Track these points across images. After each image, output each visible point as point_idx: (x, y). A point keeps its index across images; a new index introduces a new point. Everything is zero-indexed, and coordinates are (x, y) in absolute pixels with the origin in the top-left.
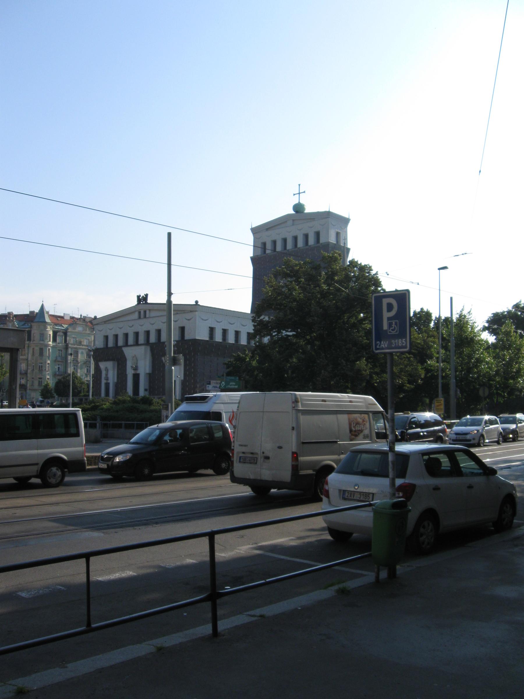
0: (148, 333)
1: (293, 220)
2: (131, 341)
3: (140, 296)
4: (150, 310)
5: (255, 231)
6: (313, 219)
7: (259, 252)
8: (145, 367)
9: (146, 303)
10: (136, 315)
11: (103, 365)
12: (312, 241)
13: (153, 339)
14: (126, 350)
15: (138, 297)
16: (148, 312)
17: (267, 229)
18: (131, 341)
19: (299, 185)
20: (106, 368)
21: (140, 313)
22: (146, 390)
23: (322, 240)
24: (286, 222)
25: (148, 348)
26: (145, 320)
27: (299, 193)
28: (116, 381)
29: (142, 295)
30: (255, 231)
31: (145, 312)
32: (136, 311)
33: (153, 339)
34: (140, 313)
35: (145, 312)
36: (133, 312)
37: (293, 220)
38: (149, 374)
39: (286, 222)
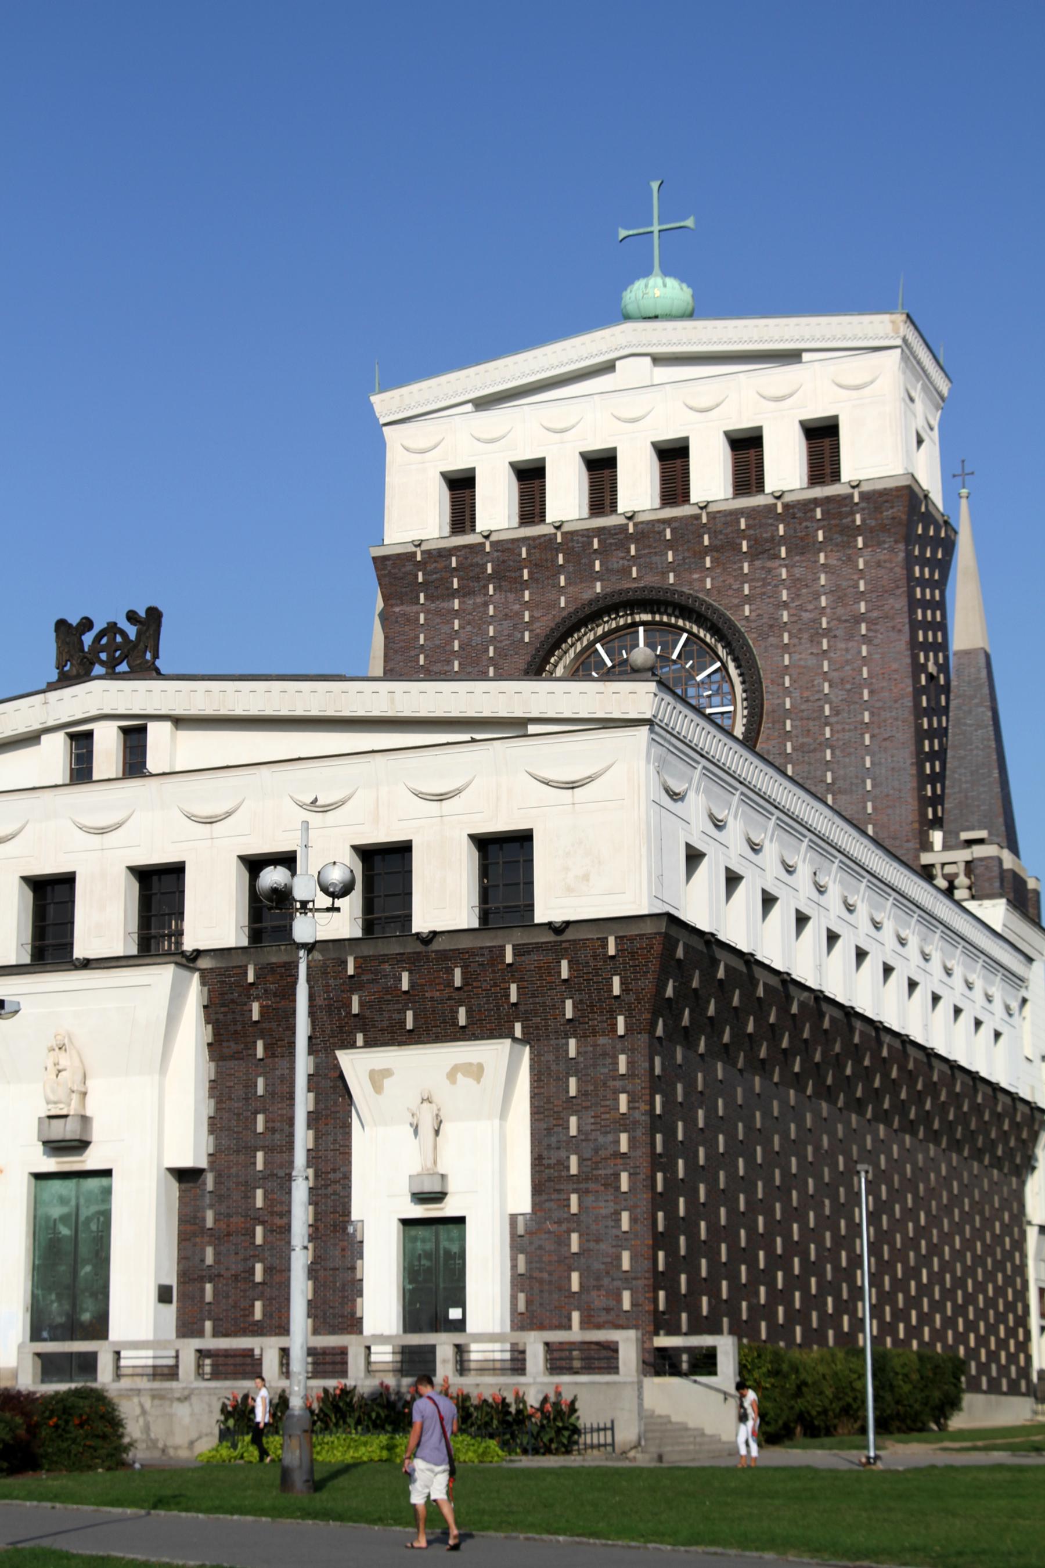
0: (159, 889)
3: (87, 624)
4: (179, 722)
6: (793, 356)
12: (785, 469)
13: (214, 918)
15: (67, 633)
17: (482, 403)
21: (82, 742)
22: (164, 1295)
24: (608, 367)
25: (194, 993)
29: (107, 609)
31: (134, 736)
33: (214, 918)
34: (82, 742)
35: (134, 736)
36: (32, 739)
38: (184, 1176)
39: (608, 367)
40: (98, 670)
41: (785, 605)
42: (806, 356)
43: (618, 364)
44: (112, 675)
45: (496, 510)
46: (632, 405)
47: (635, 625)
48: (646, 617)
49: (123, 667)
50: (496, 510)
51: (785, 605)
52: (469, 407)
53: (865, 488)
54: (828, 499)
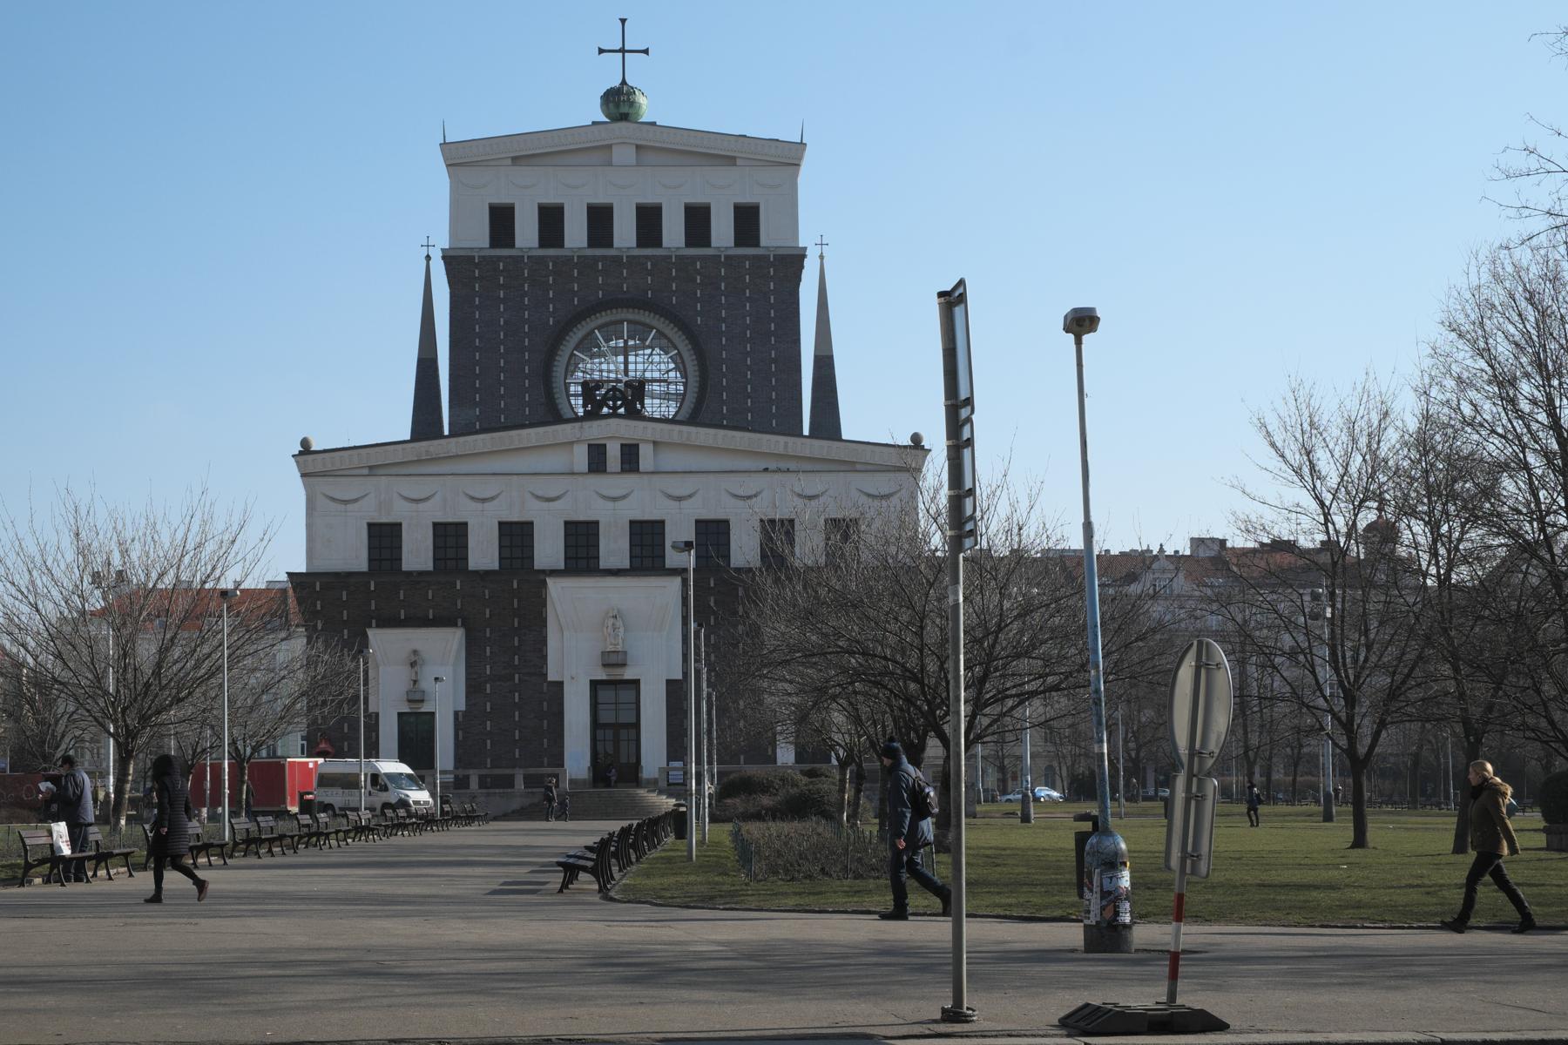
1: (638, 147)
2: (549, 550)
5: (462, 159)
6: (730, 161)
7: (479, 237)
8: (659, 656)
9: (635, 414)
10: (581, 457)
11: (386, 644)
12: (722, 232)
14: (555, 587)
16: (646, 452)
18: (549, 550)
19: (623, 21)
20: (415, 652)
23: (770, 237)
26: (630, 480)
27: (623, 51)
28: (462, 707)
30: (462, 159)
32: (578, 441)
37: (638, 147)
39: (609, 147)
40: (605, 410)
41: (724, 320)
42: (739, 162)
44: (614, 415)
45: (527, 233)
47: (621, 322)
48: (630, 317)
49: (622, 410)
50: (527, 233)
51: (724, 320)
52: (509, 162)
53: (780, 252)
54: (754, 257)
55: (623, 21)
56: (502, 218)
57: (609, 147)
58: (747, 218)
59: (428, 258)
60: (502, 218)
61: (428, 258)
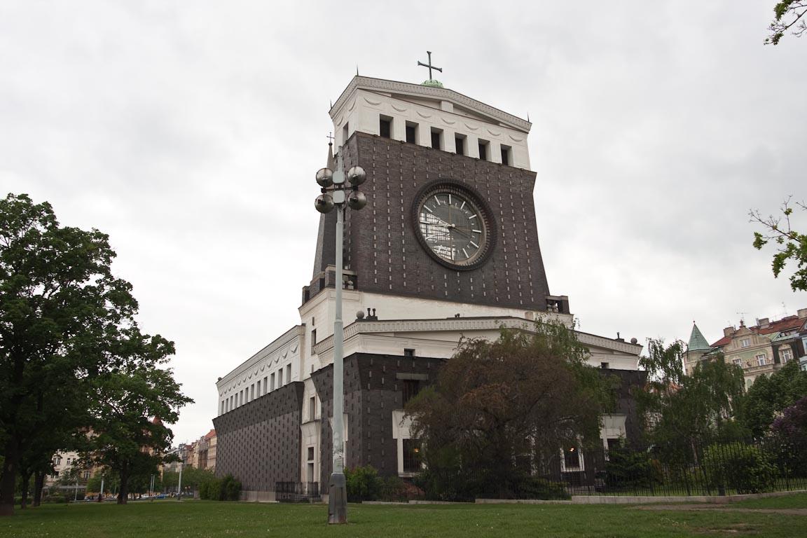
5: (362, 85)
6: (496, 123)
12: (495, 157)
17: (395, 96)
23: (516, 162)
27: (430, 67)
39: (439, 102)
43: (442, 102)
45: (399, 134)
46: (450, 118)
50: (399, 134)
52: (390, 96)
55: (429, 53)
56: (386, 123)
57: (439, 102)
58: (505, 151)
59: (331, 144)
60: (386, 123)
61: (331, 144)
